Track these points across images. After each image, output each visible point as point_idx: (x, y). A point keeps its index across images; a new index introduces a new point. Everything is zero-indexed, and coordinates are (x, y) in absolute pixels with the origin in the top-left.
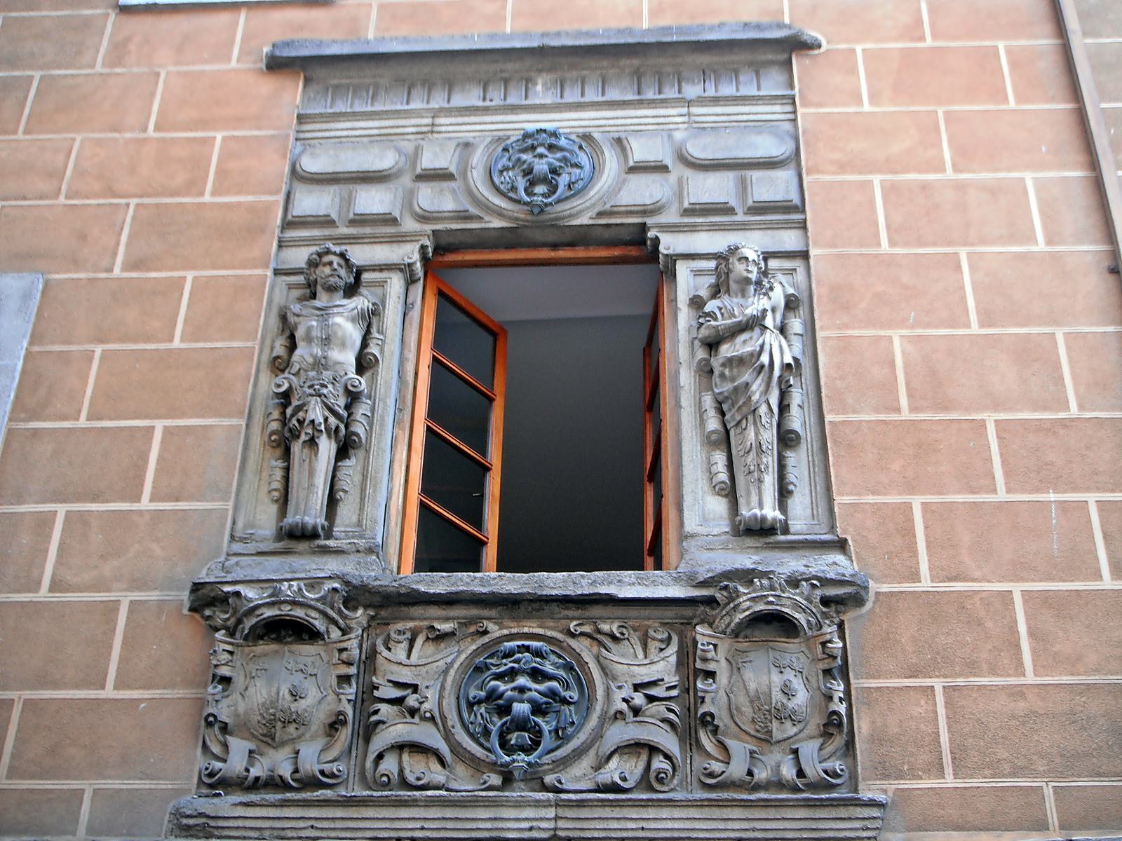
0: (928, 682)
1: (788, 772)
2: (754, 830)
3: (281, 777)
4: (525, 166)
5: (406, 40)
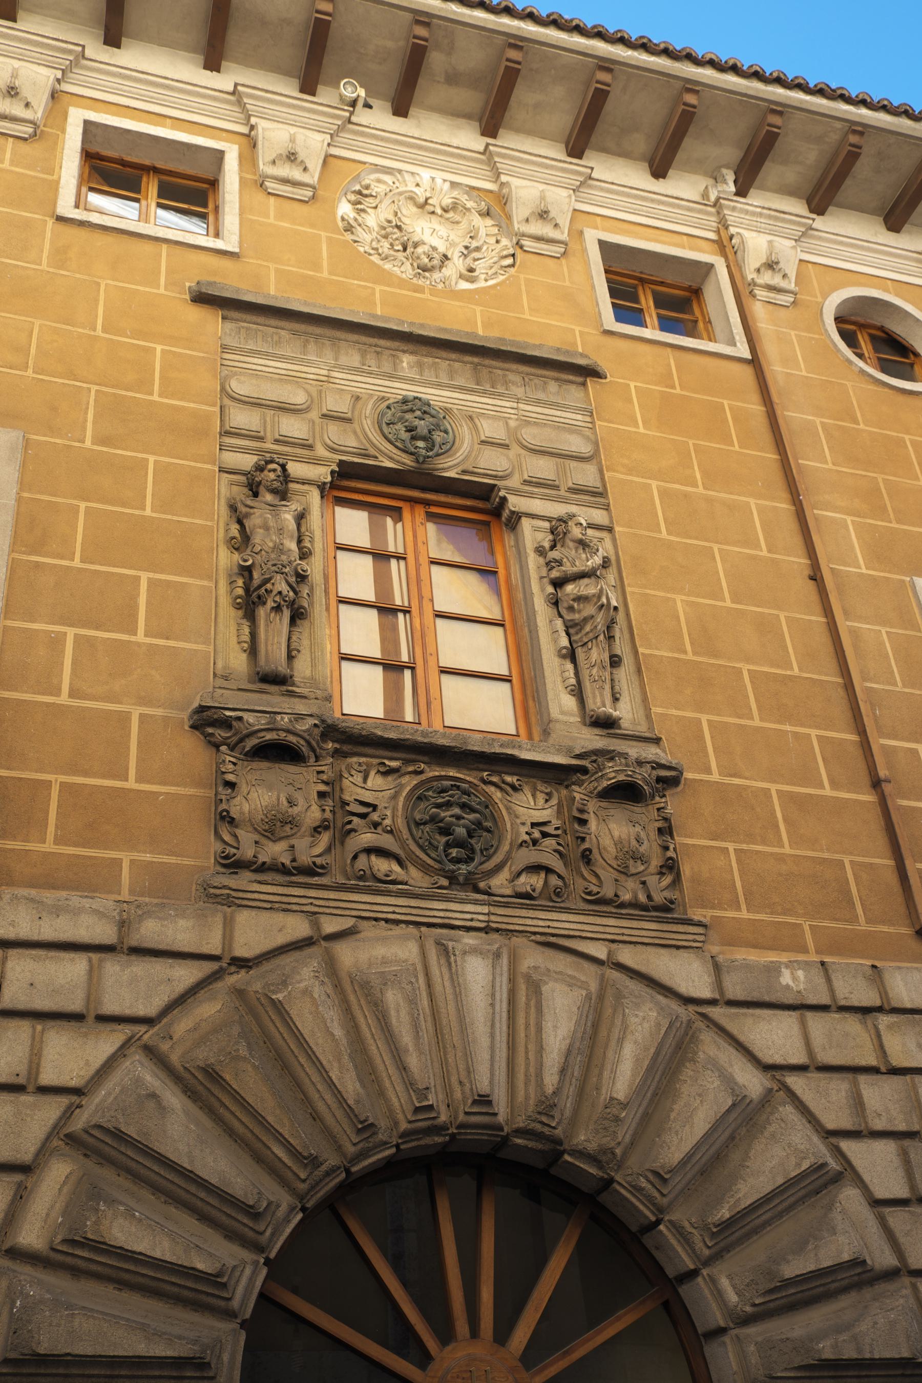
0: (724, 844)
1: (642, 898)
3: (283, 864)
5: (306, 303)
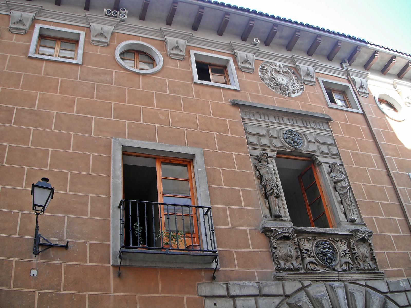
0: (383, 251)
1: (369, 267)
2: (367, 278)
3: (291, 268)
4: (291, 138)
